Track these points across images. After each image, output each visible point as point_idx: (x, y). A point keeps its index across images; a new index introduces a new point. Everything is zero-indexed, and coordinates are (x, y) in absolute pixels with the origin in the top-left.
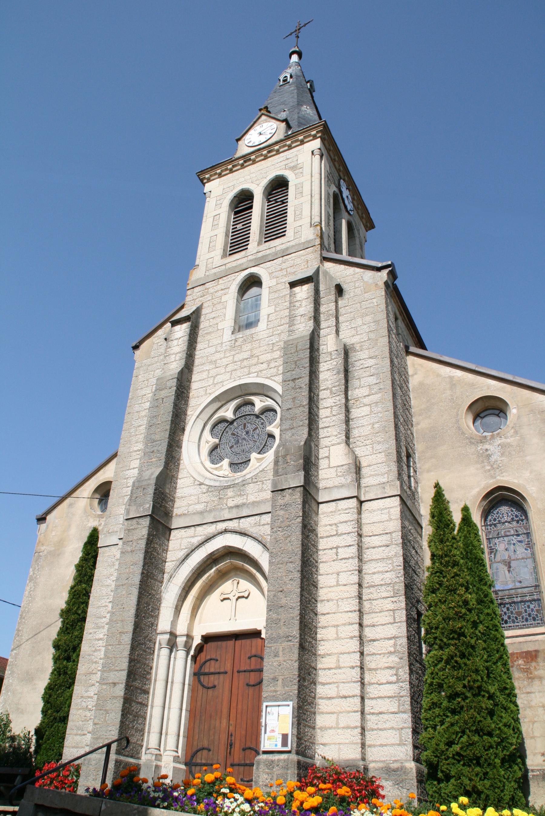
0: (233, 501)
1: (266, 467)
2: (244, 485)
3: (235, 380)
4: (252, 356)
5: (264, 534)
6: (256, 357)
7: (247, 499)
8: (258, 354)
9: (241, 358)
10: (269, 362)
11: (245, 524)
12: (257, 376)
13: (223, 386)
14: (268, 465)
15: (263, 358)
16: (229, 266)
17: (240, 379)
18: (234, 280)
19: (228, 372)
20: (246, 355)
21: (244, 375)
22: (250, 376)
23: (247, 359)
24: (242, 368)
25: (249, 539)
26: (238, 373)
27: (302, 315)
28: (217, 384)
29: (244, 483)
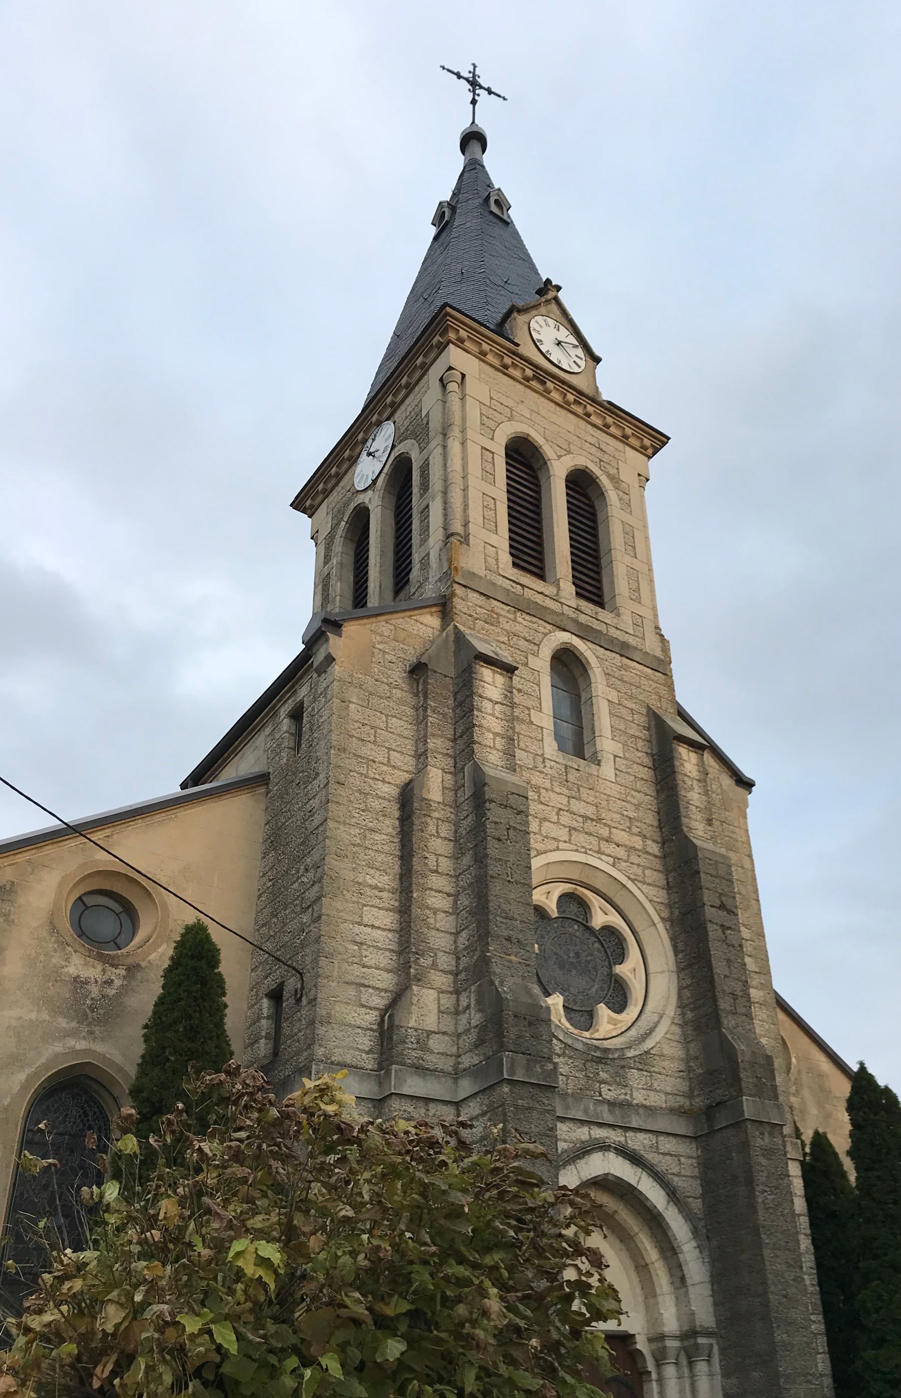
0: (609, 1090)
1: (652, 1048)
2: (623, 1067)
3: (577, 850)
4: (599, 820)
5: (667, 1170)
6: (605, 824)
7: (631, 1095)
8: (609, 823)
9: (582, 812)
10: (631, 849)
11: (638, 1142)
12: (614, 865)
13: (558, 849)
14: (654, 1047)
15: (620, 836)
16: (528, 593)
17: (586, 853)
18: (546, 635)
19: (565, 827)
20: (590, 811)
21: (590, 850)
22: (603, 857)
23: (592, 820)
24: (586, 833)
25: (644, 1173)
26: (580, 839)
27: (697, 807)
28: (546, 837)
29: (623, 1063)
